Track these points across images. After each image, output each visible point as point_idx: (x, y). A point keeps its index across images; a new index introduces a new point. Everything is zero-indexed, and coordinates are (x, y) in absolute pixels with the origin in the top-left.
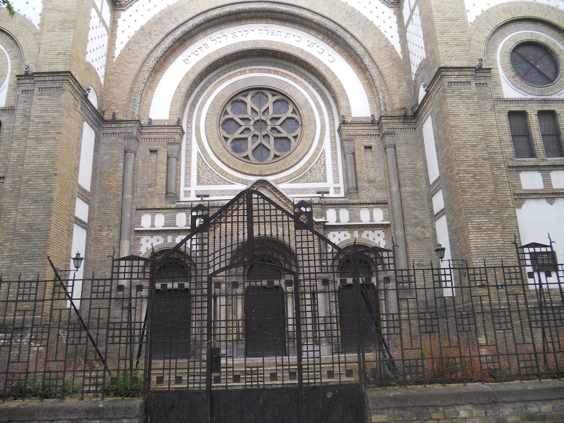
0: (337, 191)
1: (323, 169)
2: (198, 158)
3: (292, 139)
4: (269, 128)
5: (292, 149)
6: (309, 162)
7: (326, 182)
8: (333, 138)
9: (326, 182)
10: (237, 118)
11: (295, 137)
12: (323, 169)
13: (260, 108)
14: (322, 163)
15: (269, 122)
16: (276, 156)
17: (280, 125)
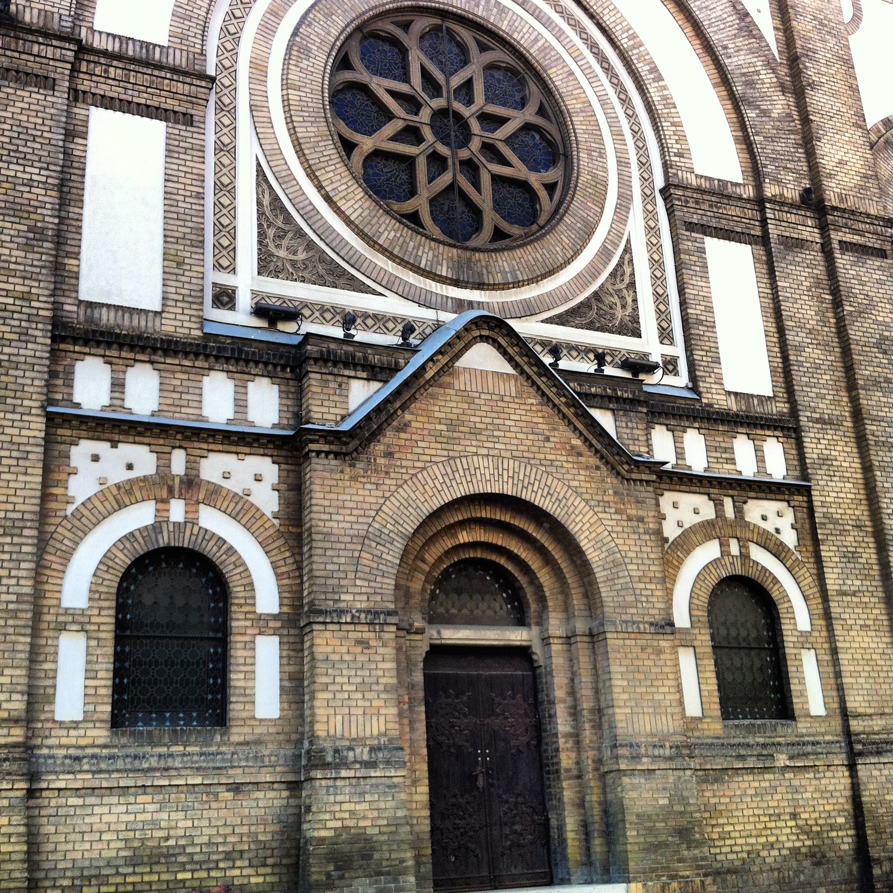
0: (671, 367)
1: (629, 300)
2: (258, 185)
3: (543, 194)
4: (475, 144)
5: (542, 220)
6: (593, 271)
7: (639, 336)
8: (650, 214)
9: (639, 336)
10: (380, 85)
11: (550, 188)
12: (629, 300)
13: (448, 75)
14: (627, 280)
15: (475, 126)
16: (499, 235)
17: (508, 141)
